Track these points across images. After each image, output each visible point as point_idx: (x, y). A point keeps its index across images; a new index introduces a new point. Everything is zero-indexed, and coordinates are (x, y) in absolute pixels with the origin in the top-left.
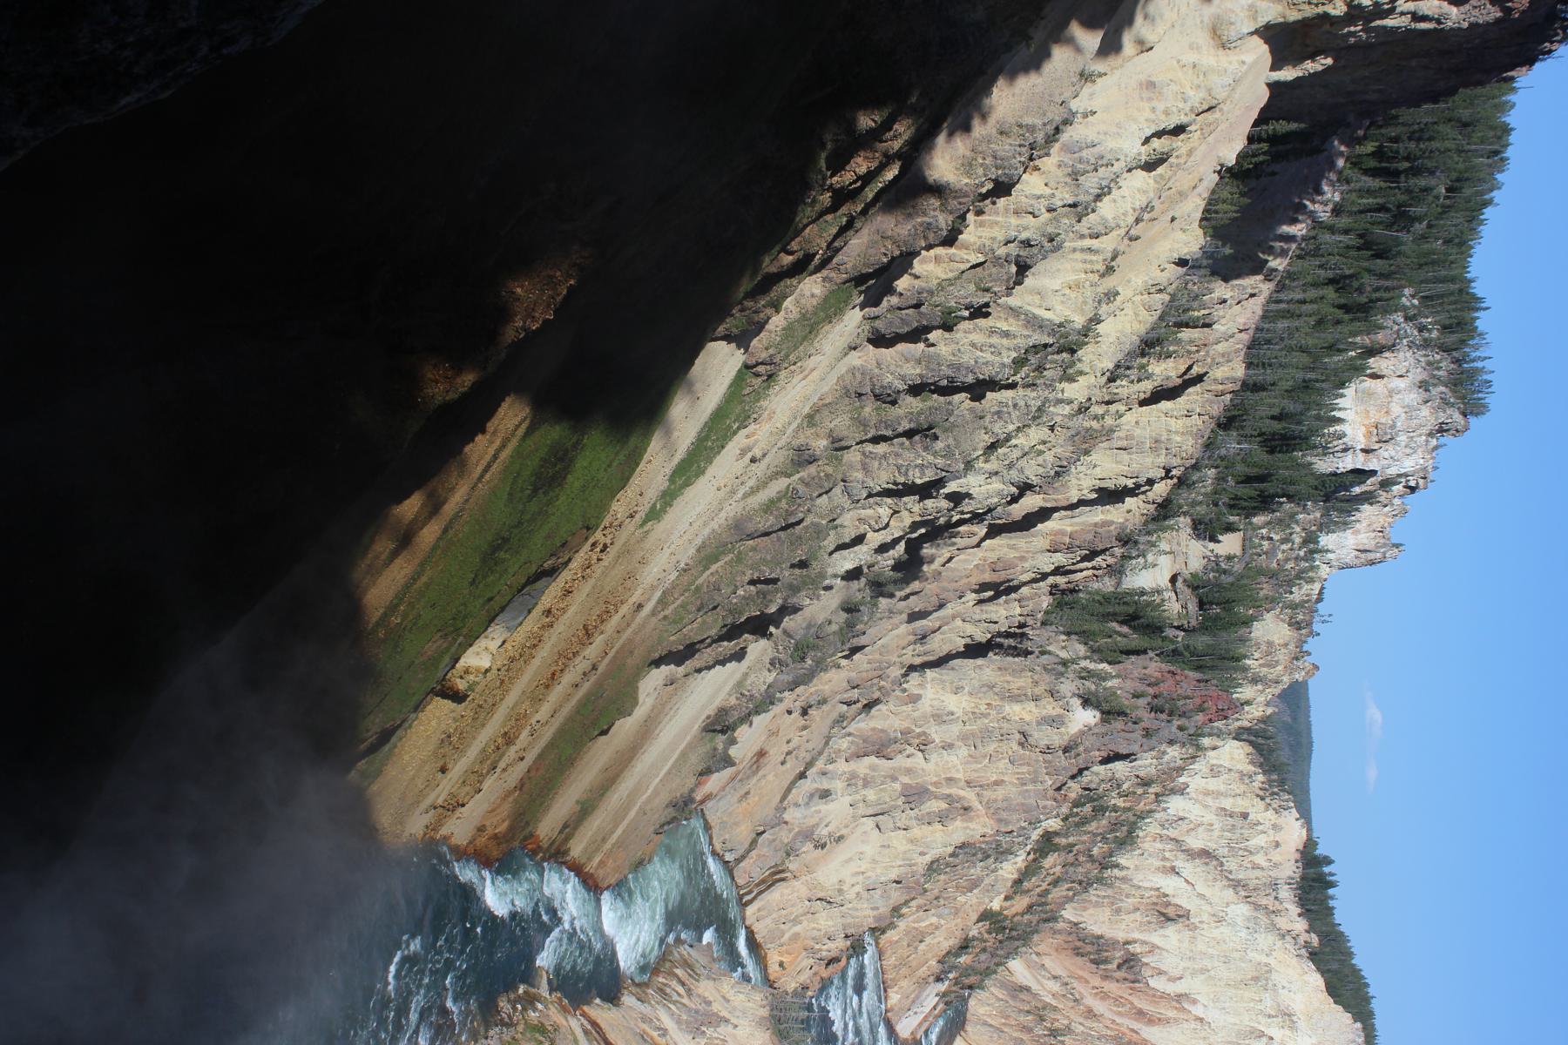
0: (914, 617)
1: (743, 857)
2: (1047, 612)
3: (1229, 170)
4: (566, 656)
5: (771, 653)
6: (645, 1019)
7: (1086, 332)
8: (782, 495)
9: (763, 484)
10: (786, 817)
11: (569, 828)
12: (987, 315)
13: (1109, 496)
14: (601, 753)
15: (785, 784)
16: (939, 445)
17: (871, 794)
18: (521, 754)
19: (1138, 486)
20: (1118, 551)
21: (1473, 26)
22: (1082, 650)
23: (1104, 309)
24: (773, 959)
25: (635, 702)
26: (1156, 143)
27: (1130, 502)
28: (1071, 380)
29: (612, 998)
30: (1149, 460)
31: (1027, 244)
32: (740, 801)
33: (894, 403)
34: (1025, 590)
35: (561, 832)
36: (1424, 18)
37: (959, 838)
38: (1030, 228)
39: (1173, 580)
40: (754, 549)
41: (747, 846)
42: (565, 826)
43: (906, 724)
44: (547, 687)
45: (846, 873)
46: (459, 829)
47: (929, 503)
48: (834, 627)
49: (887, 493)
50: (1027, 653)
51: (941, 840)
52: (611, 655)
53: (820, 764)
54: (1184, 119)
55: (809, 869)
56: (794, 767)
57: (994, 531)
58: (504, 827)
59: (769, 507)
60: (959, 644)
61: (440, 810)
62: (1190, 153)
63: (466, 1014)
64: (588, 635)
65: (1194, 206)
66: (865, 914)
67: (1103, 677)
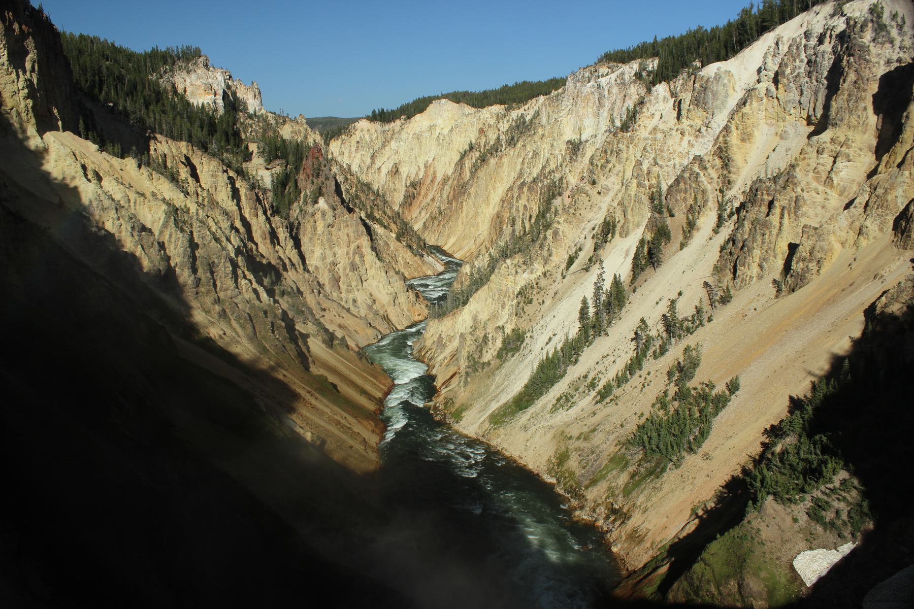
0: (286, 270)
2: (282, 217)
3: (100, 147)
6: (441, 365)
7: (168, 204)
8: (238, 322)
11: (370, 397)
12: (163, 243)
13: (235, 194)
14: (343, 388)
16: (216, 261)
17: (354, 284)
19: (231, 183)
20: (257, 191)
21: (36, 48)
22: (296, 204)
23: (160, 197)
24: (417, 318)
25: (322, 376)
26: (90, 177)
27: (237, 185)
28: (189, 209)
29: (433, 378)
30: (220, 179)
31: (133, 228)
33: (200, 279)
34: (273, 226)
36: (33, 67)
37: (369, 250)
38: (126, 228)
39: (268, 169)
43: (327, 271)
45: (384, 292)
46: (373, 439)
47: (240, 264)
48: (290, 300)
49: (236, 281)
50: (299, 224)
51: (370, 256)
53: (343, 303)
54: (79, 165)
55: (383, 306)
56: (344, 314)
57: (251, 238)
58: (372, 423)
59: (243, 327)
60: (295, 251)
62: (94, 163)
63: (441, 432)
65: (116, 161)
66: (399, 285)
67: (306, 196)
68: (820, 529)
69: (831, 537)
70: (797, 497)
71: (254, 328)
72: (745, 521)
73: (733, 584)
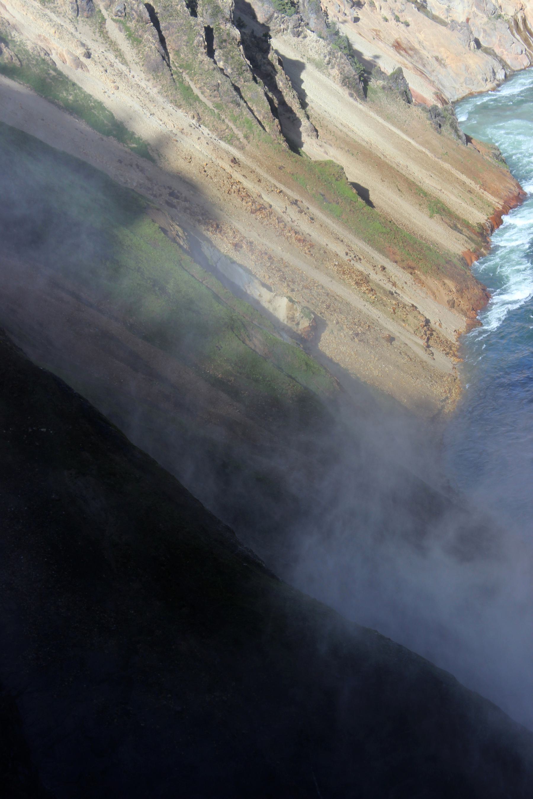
1: (501, 61)
4: (283, 228)
5: (288, 36)
9: (113, 46)
10: (462, 19)
15: (428, 21)
18: (379, 269)
25: (329, 164)
32: (445, 66)
35: (460, 232)
40: (177, 53)
41: (489, 58)
42: (455, 228)
44: (312, 246)
46: (451, 324)
52: (283, 188)
59: (135, 39)
61: (431, 342)
64: (262, 208)
71: (162, 40)
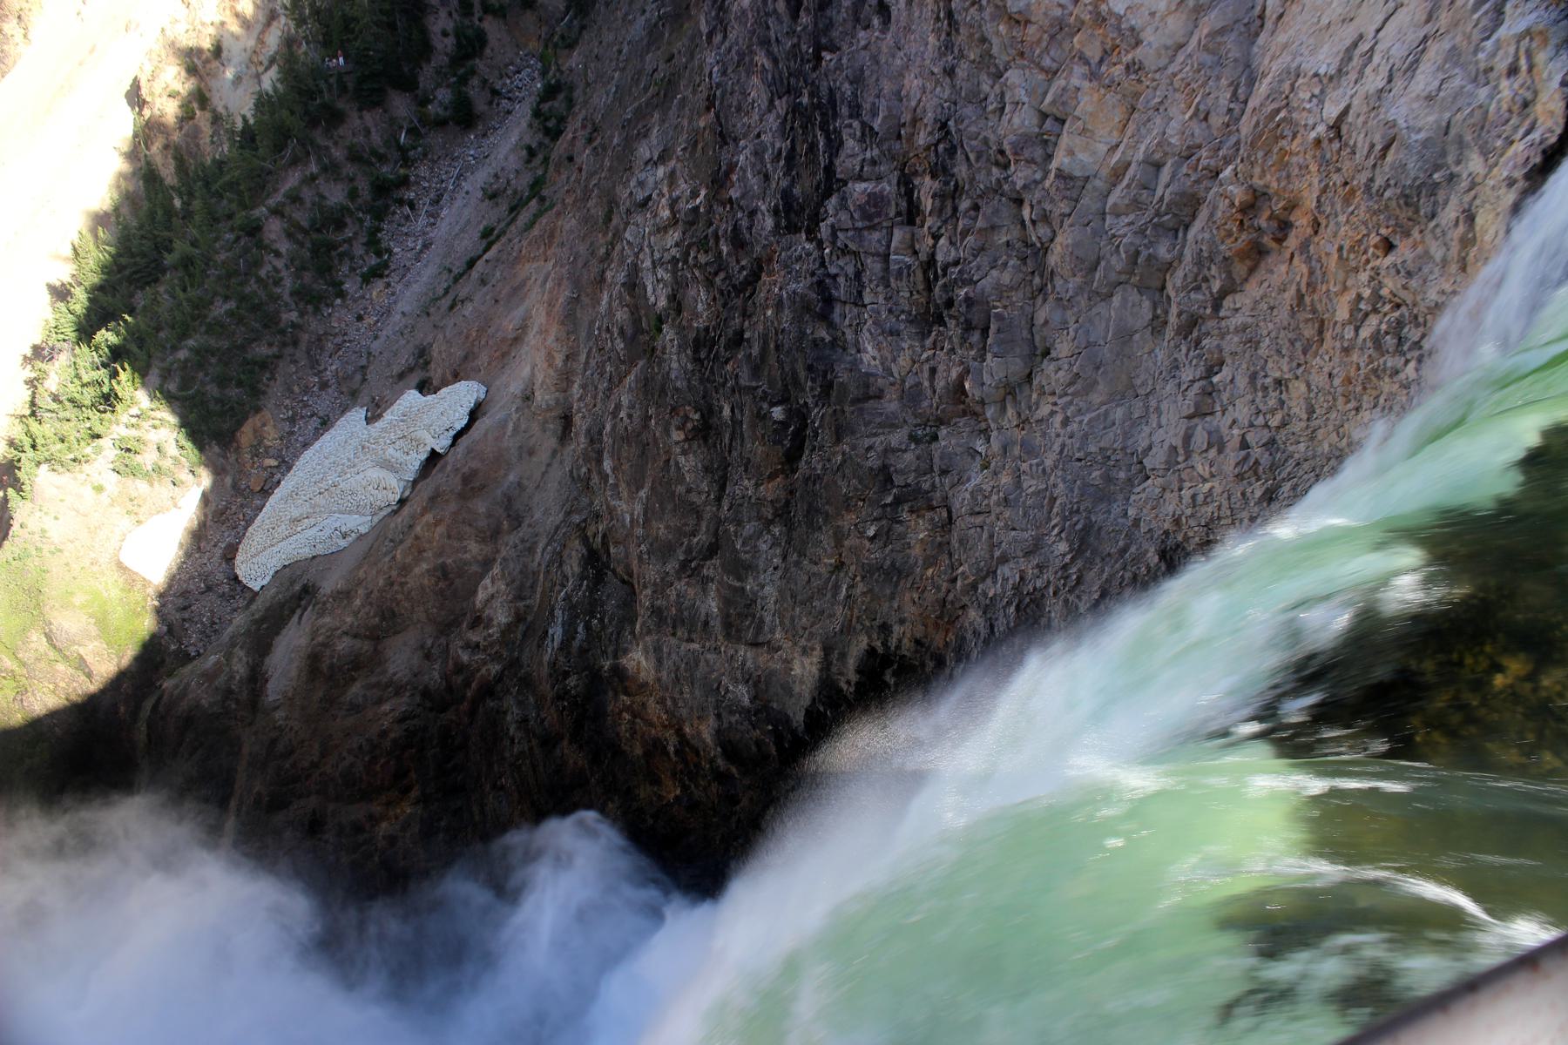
68: (141, 486)
69: (163, 490)
70: (88, 450)
72: (15, 529)
73: (37, 640)
